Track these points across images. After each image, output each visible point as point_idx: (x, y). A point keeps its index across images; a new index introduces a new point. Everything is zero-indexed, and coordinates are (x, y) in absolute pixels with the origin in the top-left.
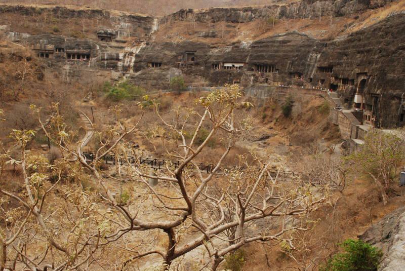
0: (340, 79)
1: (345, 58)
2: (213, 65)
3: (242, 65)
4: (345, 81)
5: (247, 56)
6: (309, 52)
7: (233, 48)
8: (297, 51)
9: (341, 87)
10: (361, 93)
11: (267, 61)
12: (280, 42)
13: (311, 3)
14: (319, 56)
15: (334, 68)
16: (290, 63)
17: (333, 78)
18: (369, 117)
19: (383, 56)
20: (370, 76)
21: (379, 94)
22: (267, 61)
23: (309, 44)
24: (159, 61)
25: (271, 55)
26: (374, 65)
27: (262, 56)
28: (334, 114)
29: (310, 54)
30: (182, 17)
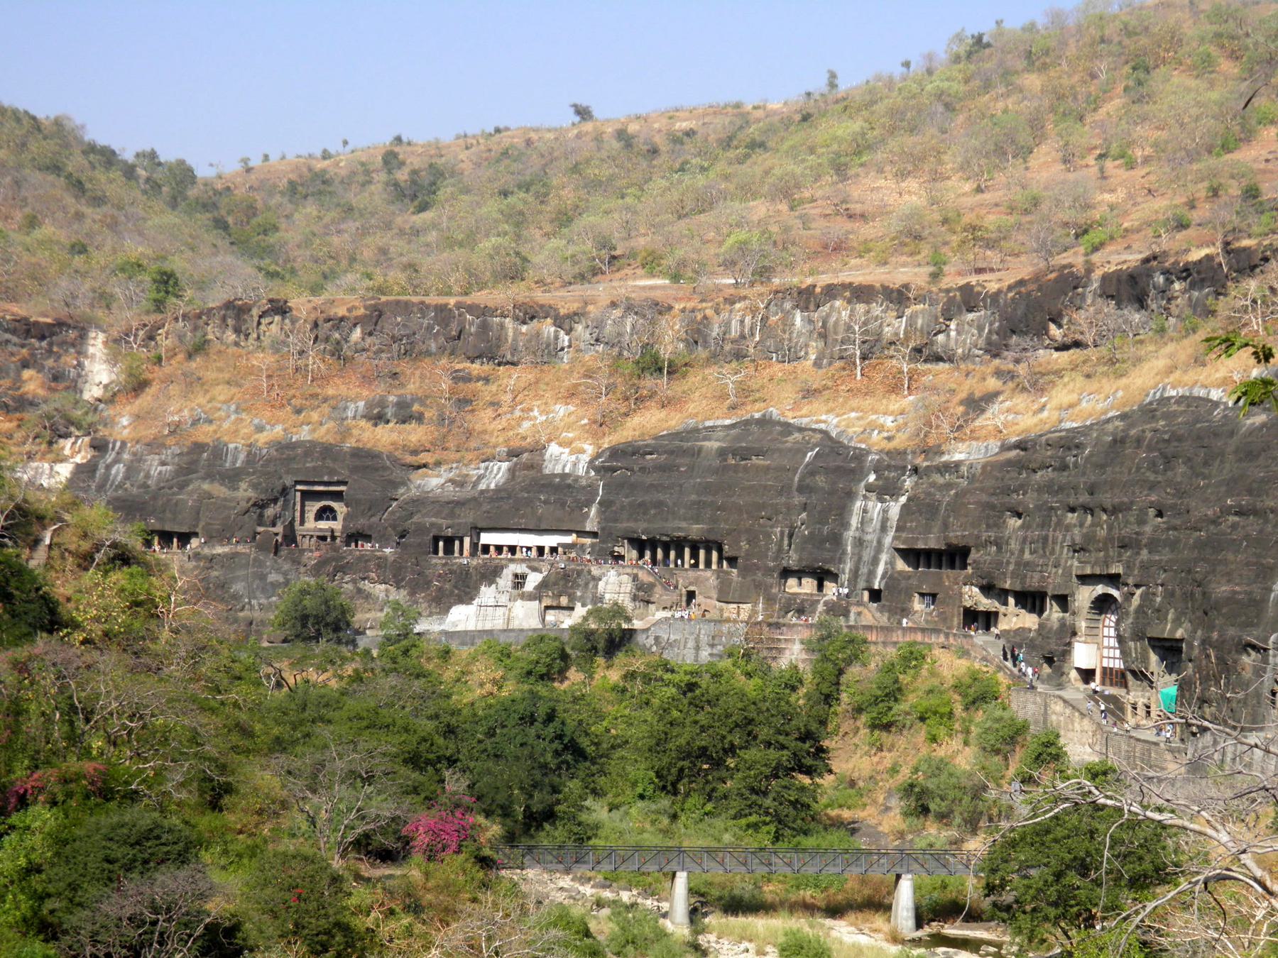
1: (1014, 523)
2: (436, 539)
6: (850, 495)
7: (512, 471)
8: (802, 489)
11: (684, 525)
12: (722, 453)
13: (812, 307)
14: (895, 509)
15: (973, 556)
16: (782, 533)
17: (976, 590)
20: (1137, 586)
22: (684, 525)
23: (840, 466)
25: (694, 503)
26: (1145, 552)
27: (659, 505)
28: (1031, 707)
29: (858, 504)
30: (237, 331)
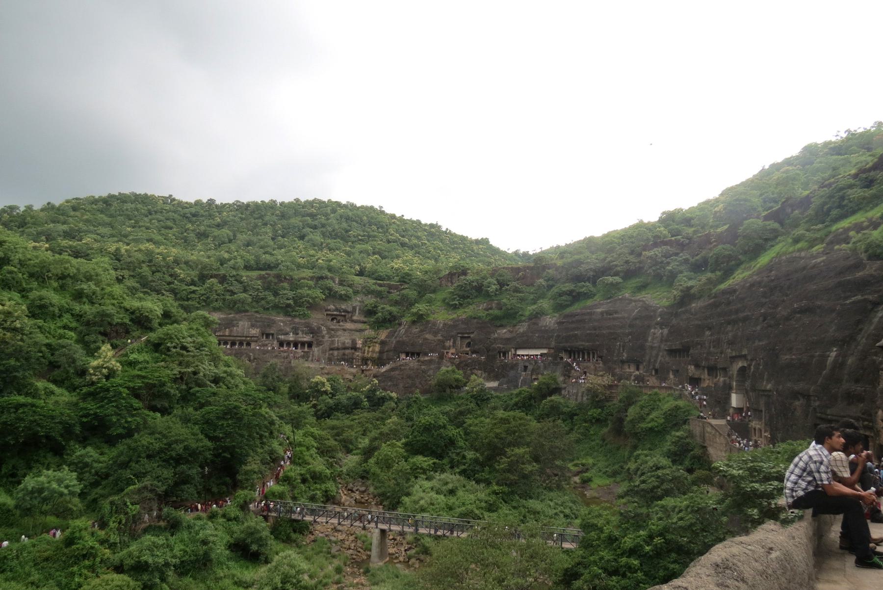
0: (704, 367)
1: (708, 333)
3: (545, 351)
4: (712, 370)
5: (552, 337)
6: (649, 327)
9: (707, 382)
10: (740, 390)
14: (666, 331)
15: (691, 351)
18: (760, 430)
19: (770, 326)
20: (752, 360)
21: (770, 391)
24: (417, 350)
26: (757, 342)
